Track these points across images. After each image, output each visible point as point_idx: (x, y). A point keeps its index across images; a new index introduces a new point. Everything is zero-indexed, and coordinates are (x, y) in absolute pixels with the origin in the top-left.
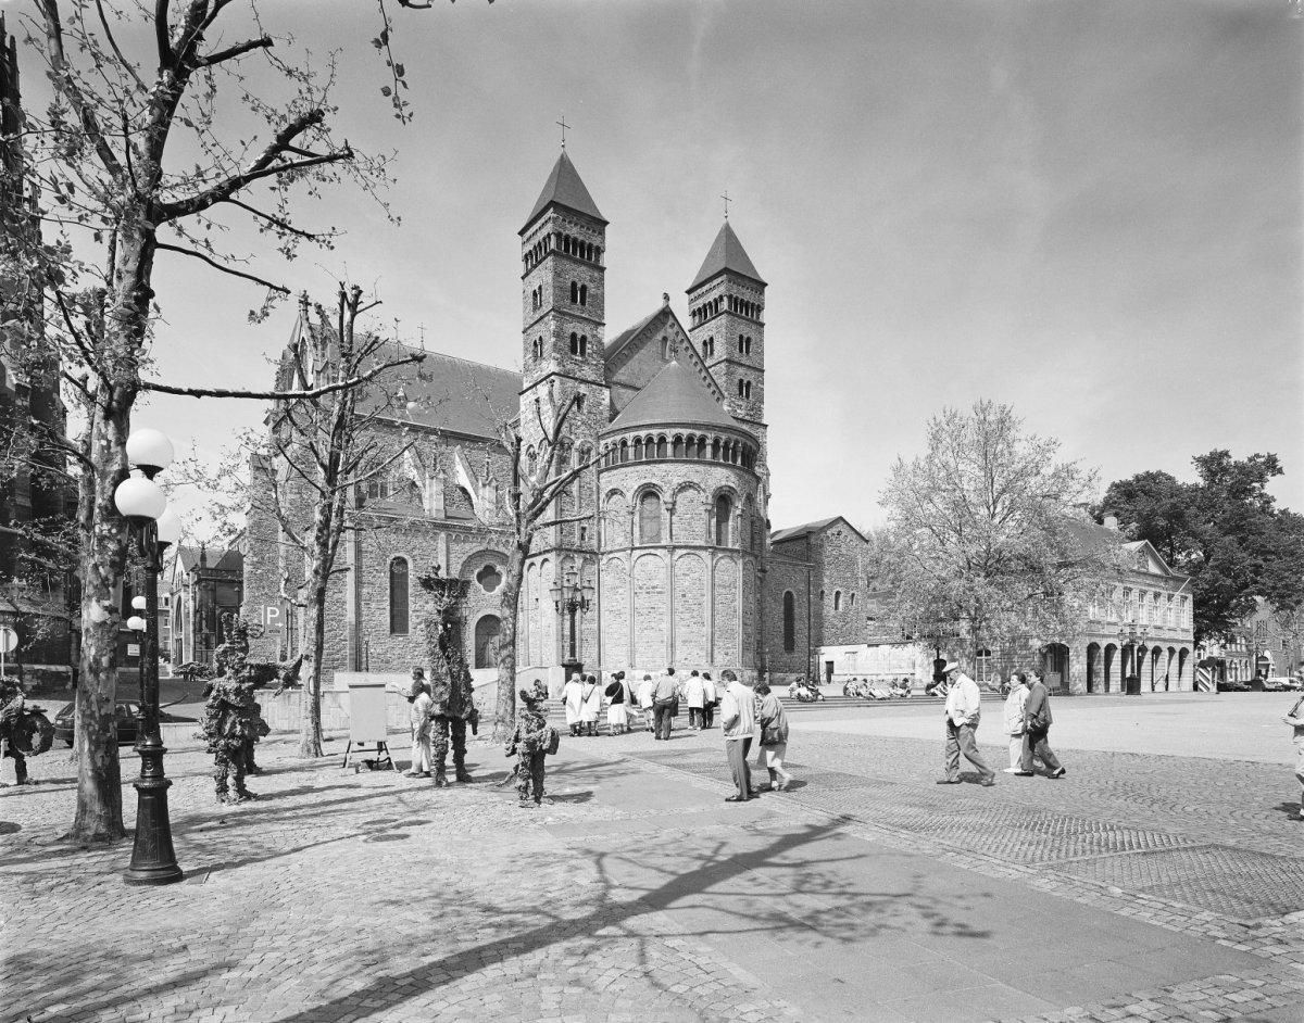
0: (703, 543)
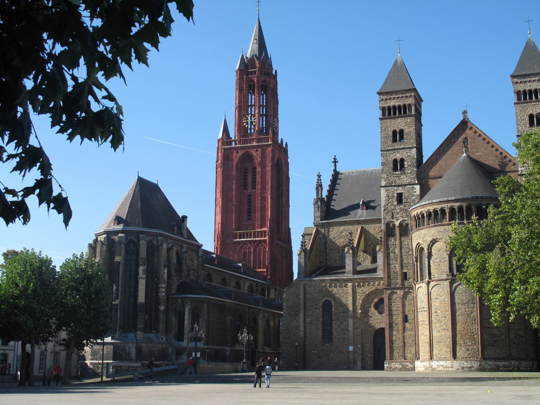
0: (445, 277)
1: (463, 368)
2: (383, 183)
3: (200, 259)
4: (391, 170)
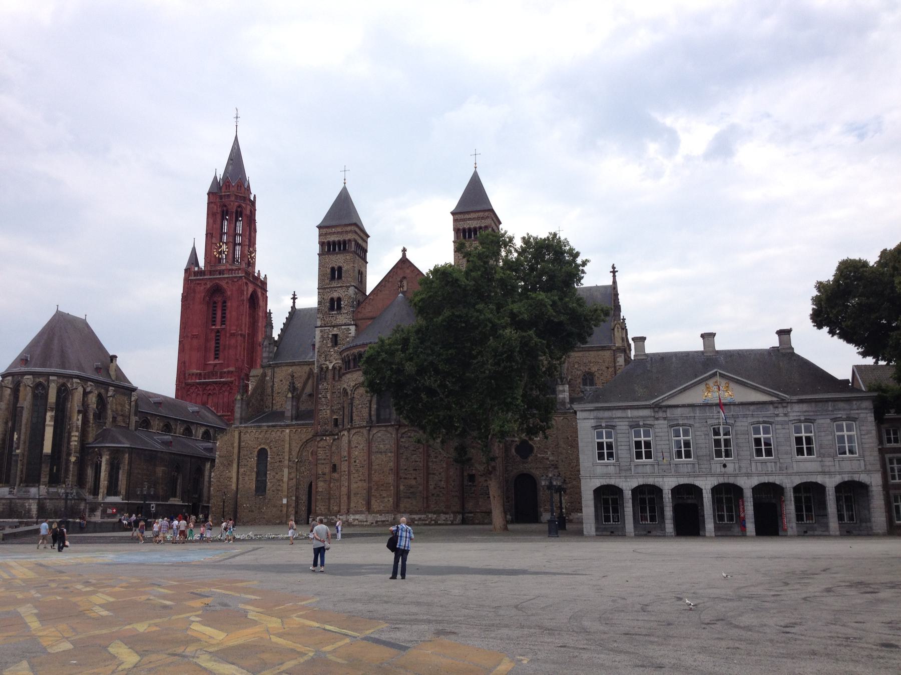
0: (365, 424)
1: (377, 522)
2: (319, 323)
3: (133, 403)
4: (327, 310)
